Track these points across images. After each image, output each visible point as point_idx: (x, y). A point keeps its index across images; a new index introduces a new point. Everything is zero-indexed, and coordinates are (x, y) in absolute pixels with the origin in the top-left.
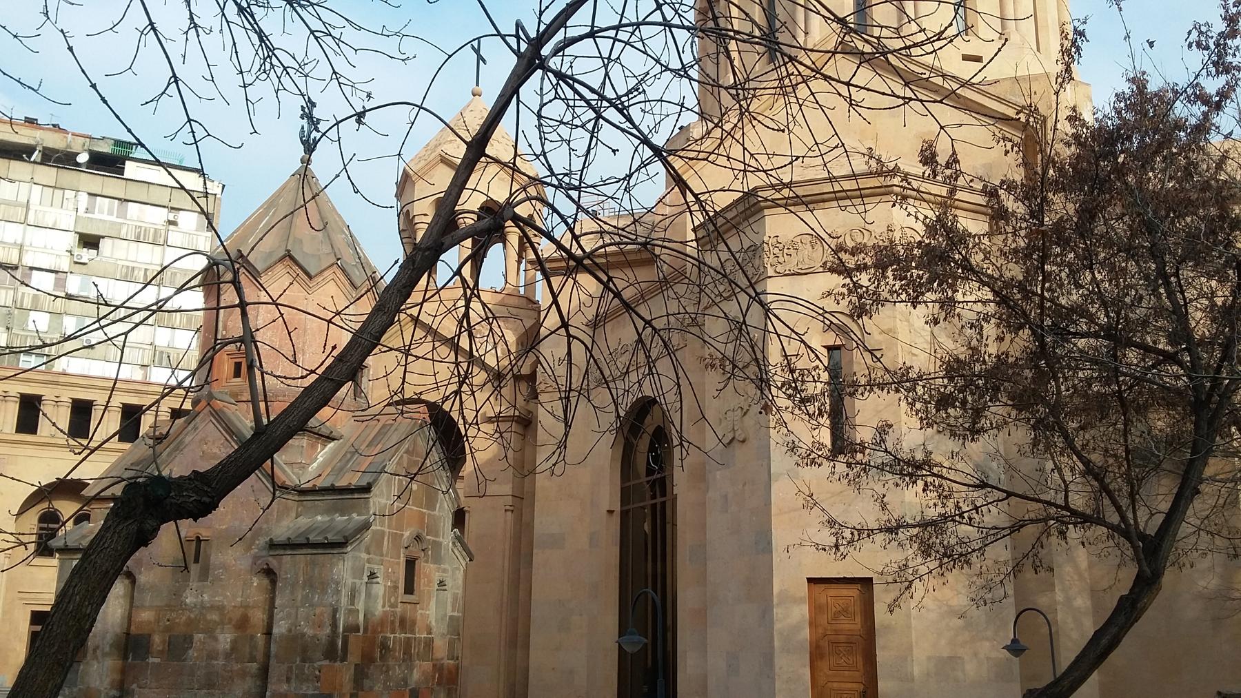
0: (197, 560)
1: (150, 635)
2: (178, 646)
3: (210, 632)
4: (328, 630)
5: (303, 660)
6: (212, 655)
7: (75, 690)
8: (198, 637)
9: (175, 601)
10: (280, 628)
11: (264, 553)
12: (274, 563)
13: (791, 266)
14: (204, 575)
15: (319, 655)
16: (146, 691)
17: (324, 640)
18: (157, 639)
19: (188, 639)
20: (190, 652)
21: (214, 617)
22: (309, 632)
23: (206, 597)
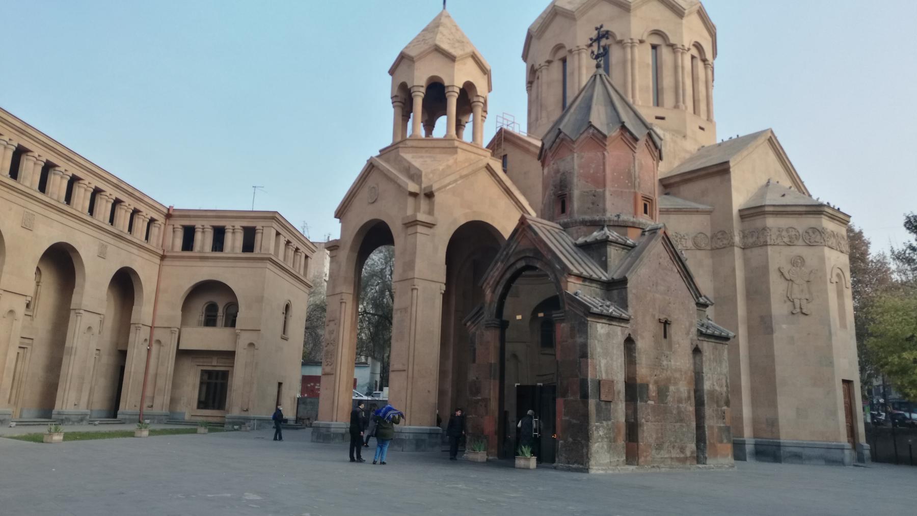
0: (665, 337)
1: (648, 385)
2: (662, 393)
3: (675, 384)
4: (725, 389)
5: (718, 406)
6: (680, 401)
7: (610, 423)
8: (672, 388)
9: (657, 364)
10: (707, 386)
11: (696, 338)
12: (700, 347)
13: (830, 243)
14: (670, 346)
15: (723, 403)
16: (649, 424)
17: (724, 394)
18: (651, 386)
19: (667, 390)
20: (670, 398)
21: (677, 375)
22: (717, 388)
23: (673, 363)
